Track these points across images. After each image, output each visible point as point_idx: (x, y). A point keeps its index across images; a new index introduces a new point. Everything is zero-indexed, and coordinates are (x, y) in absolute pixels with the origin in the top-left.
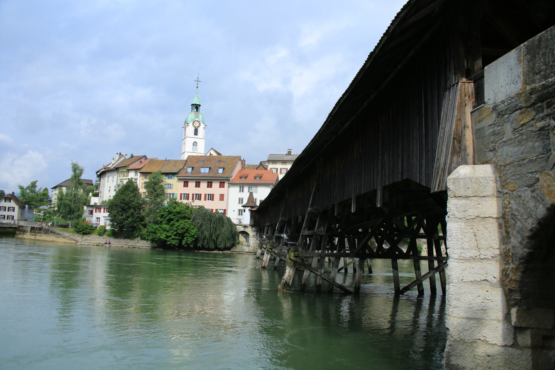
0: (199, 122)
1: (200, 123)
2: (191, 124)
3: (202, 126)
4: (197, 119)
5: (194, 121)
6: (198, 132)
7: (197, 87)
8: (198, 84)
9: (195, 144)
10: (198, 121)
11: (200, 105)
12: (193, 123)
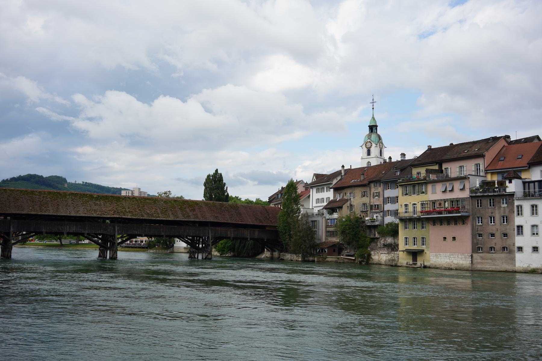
0: (371, 142)
1: (371, 144)
2: (364, 146)
4: (369, 140)
5: (366, 143)
6: (371, 152)
7: (373, 109)
8: (373, 105)
12: (366, 144)
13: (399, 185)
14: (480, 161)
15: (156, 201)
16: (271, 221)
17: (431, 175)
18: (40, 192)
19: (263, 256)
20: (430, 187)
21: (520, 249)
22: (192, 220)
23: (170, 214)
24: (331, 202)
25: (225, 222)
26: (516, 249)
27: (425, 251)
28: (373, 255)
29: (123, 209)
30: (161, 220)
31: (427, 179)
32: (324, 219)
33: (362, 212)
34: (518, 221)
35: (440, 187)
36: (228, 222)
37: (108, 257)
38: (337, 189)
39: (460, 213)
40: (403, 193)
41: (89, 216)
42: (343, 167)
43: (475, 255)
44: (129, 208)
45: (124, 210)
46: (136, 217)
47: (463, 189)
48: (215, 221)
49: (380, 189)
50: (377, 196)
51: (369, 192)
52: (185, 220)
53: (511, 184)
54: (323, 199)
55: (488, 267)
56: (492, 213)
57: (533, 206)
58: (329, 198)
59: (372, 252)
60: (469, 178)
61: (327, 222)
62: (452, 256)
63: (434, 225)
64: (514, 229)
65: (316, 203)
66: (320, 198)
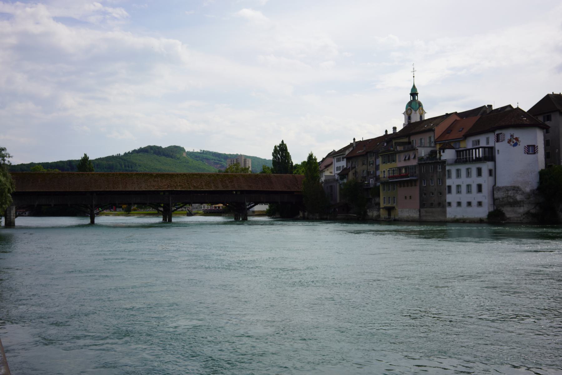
7: (414, 77)
8: (414, 74)
13: (381, 155)
14: (431, 134)
15: (202, 176)
16: (298, 187)
17: (398, 147)
18: (113, 174)
19: (299, 217)
20: (397, 155)
21: (450, 204)
22: (230, 189)
23: (212, 185)
24: (344, 170)
25: (258, 189)
26: (447, 205)
27: (396, 207)
28: (369, 212)
29: (175, 183)
30: (205, 191)
31: (396, 150)
32: (338, 184)
33: (363, 177)
34: (448, 182)
35: (402, 156)
36: (260, 190)
37: (167, 221)
38: (349, 159)
39: (409, 177)
40: (382, 162)
41: (148, 190)
43: (422, 210)
44: (180, 183)
45: (176, 184)
46: (185, 190)
47: (415, 158)
48: (249, 189)
49: (373, 158)
50: (371, 164)
52: (224, 190)
53: (444, 153)
54: (340, 167)
55: (429, 218)
56: (432, 176)
57: (468, 169)
58: (344, 166)
59: (368, 210)
60: (417, 149)
61: (340, 186)
62: (409, 211)
63: (400, 187)
64: (446, 189)
65: (337, 171)
66: (339, 166)
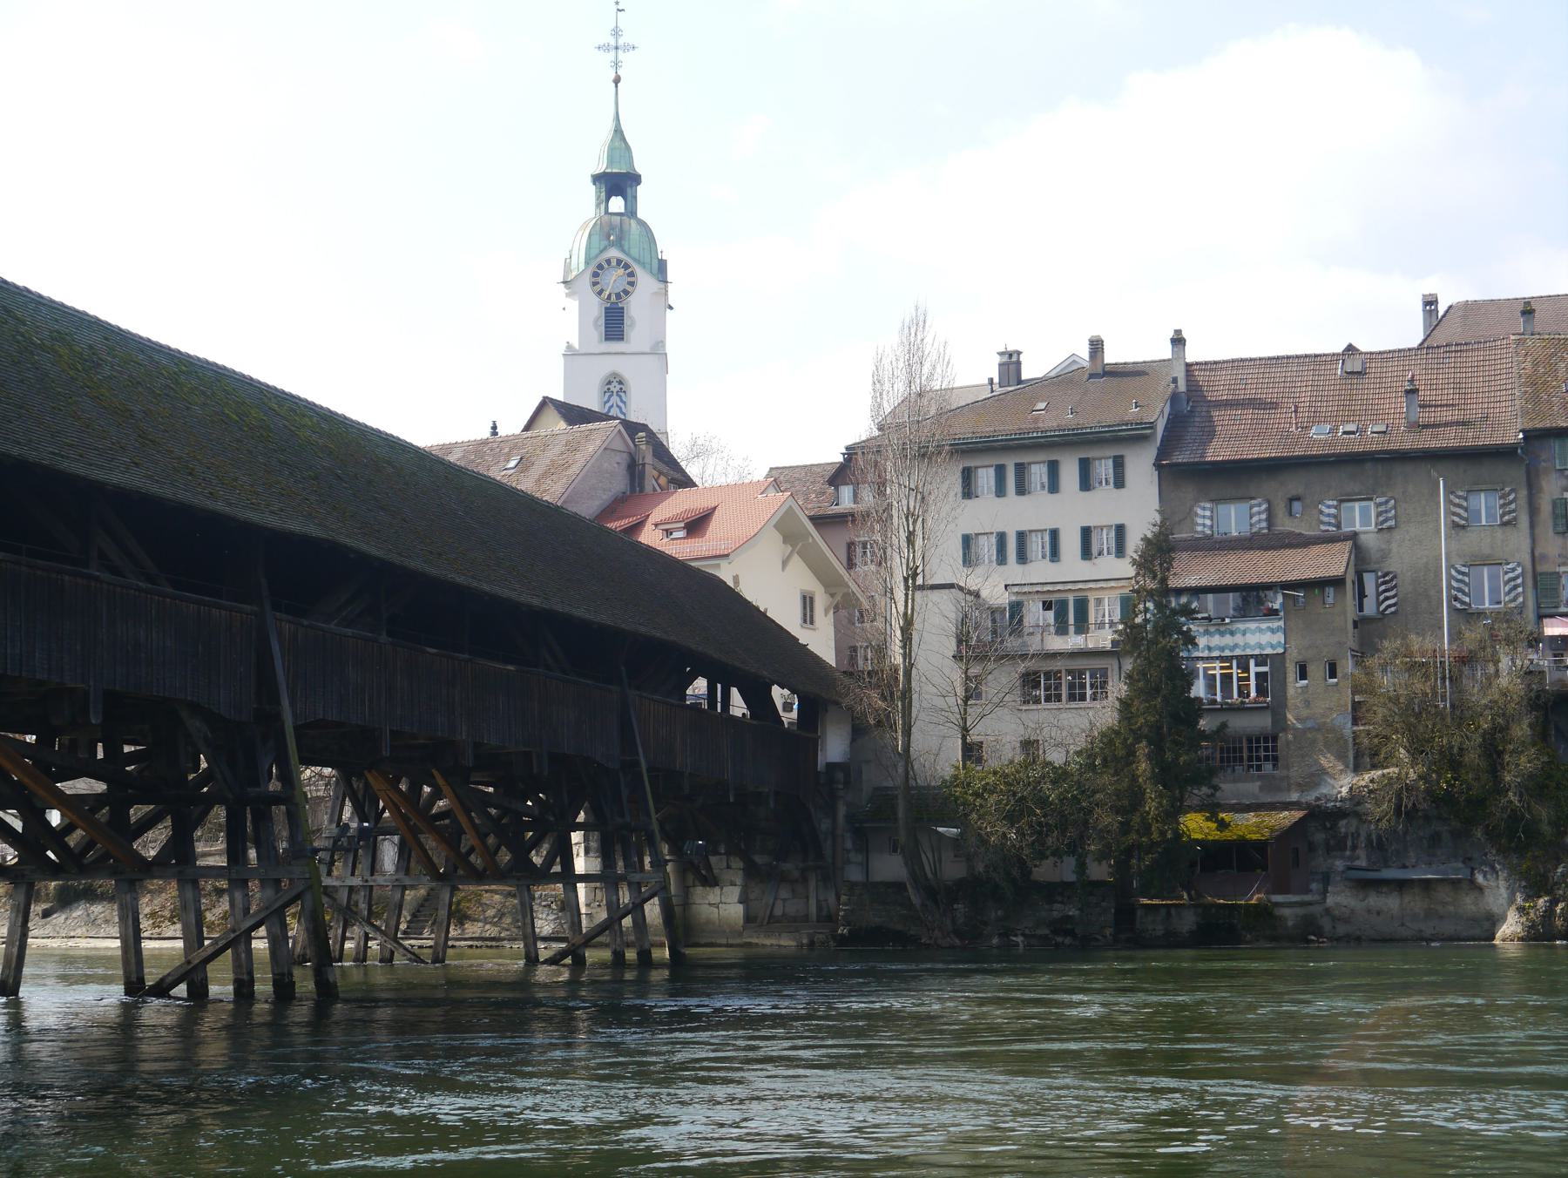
0: (627, 266)
1: (632, 274)
3: (645, 281)
4: (614, 253)
5: (600, 267)
7: (617, 81)
8: (616, 64)
9: (615, 387)
10: (619, 262)
11: (635, 179)
12: (595, 275)
42: (1096, 346)
51: (1523, 493)
